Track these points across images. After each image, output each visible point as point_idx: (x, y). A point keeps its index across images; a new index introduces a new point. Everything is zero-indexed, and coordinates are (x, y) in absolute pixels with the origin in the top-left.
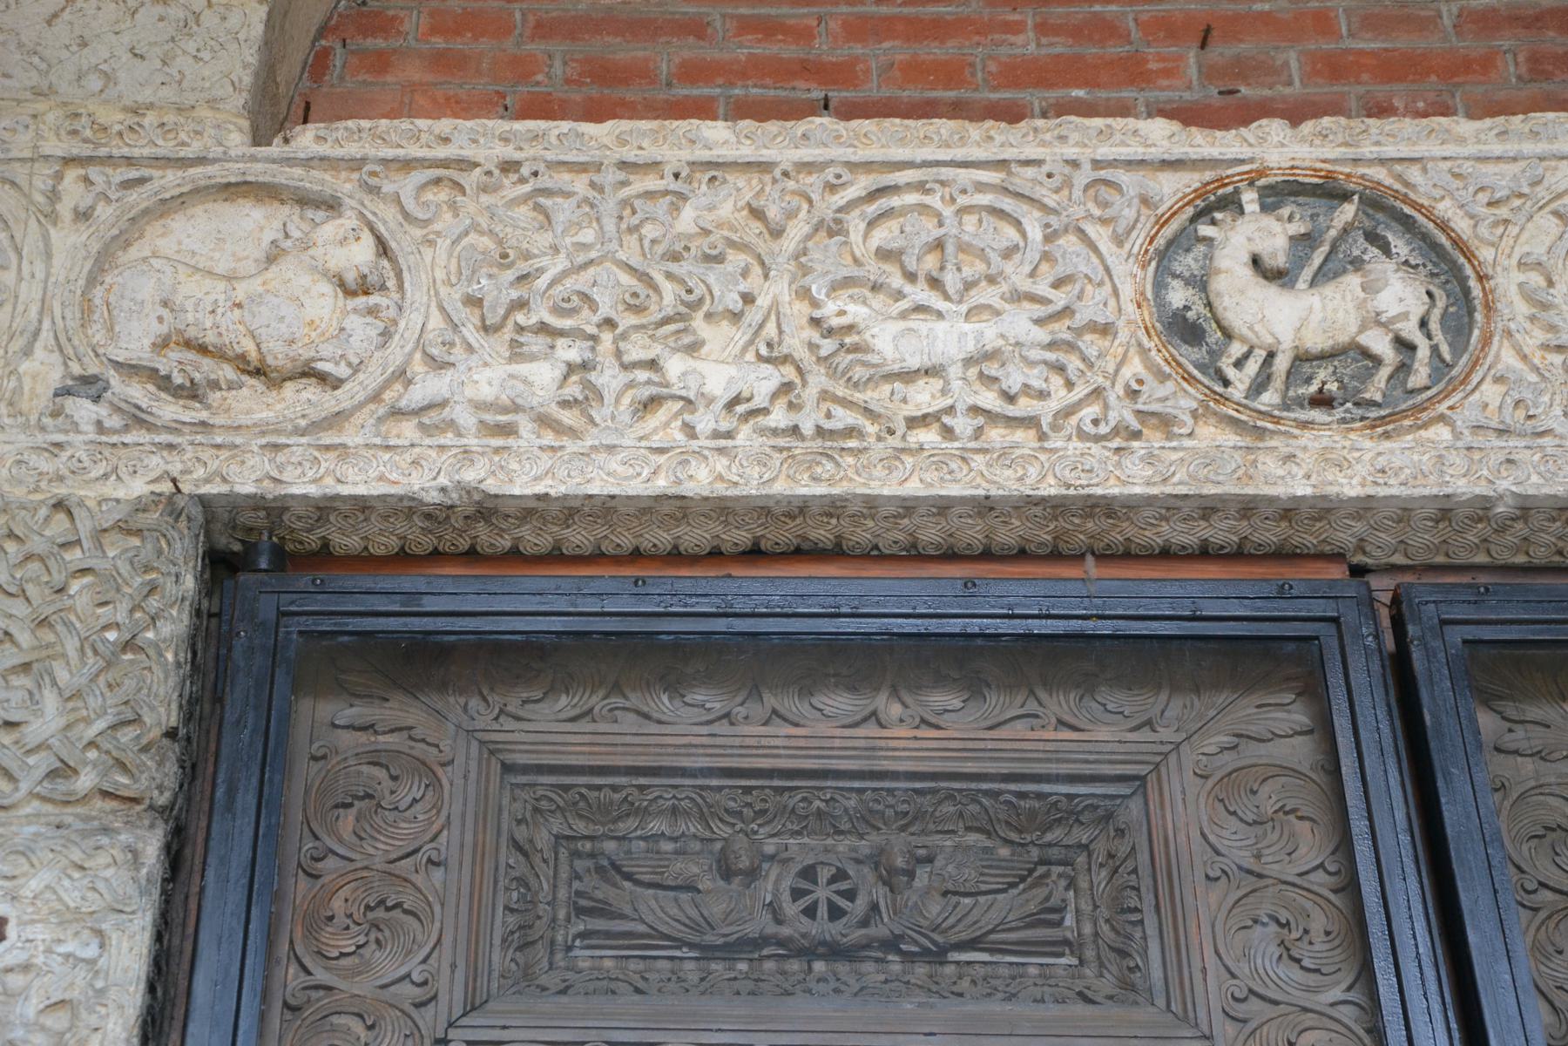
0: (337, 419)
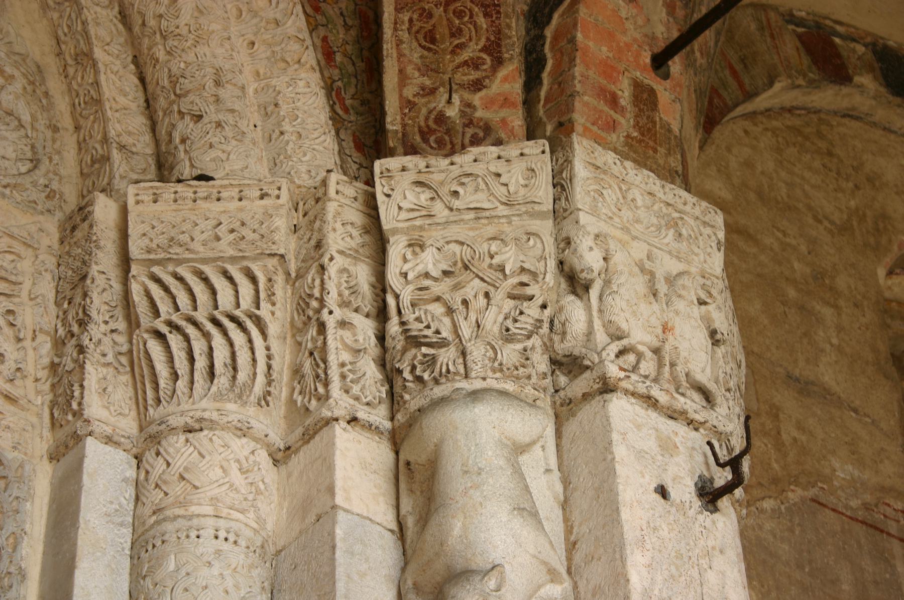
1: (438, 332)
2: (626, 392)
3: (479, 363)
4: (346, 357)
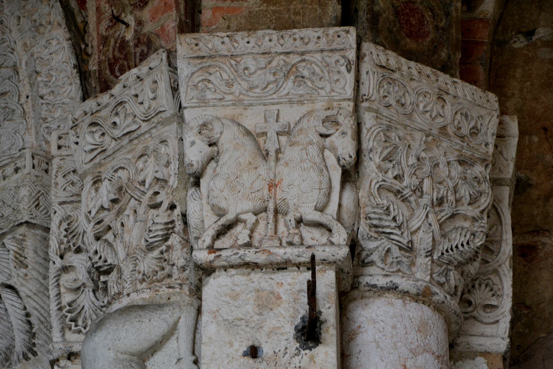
1: (106, 261)
2: (225, 269)
3: (128, 280)
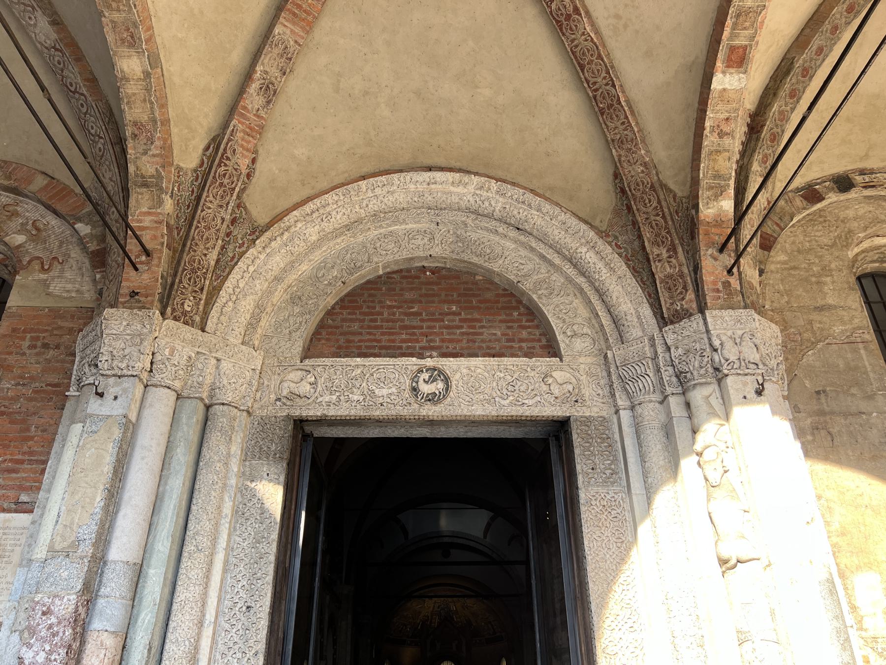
0: (309, 404)
4: (668, 378)
